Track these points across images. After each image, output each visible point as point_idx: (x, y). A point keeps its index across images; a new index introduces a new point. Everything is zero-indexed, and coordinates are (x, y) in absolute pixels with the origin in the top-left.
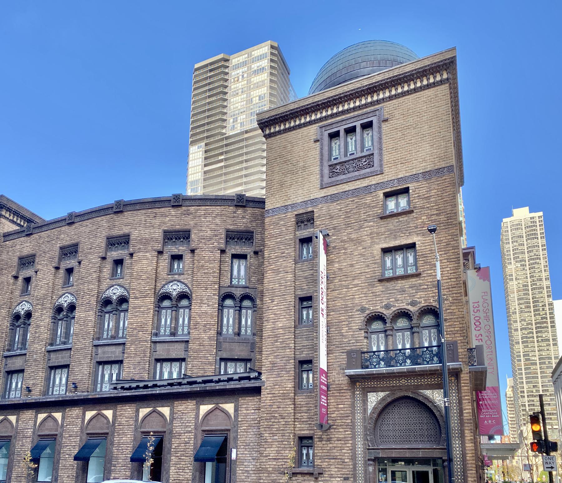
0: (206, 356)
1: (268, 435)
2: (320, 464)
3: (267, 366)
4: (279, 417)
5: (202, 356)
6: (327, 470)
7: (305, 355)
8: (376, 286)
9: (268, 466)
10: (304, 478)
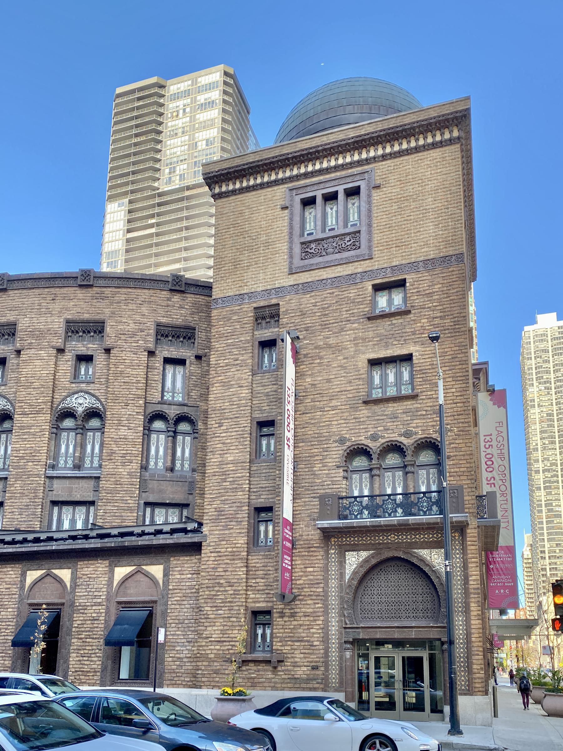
0: (125, 498)
1: (209, 609)
2: (280, 648)
3: (210, 514)
4: (225, 584)
5: (119, 498)
6: (289, 656)
7: (263, 500)
8: (361, 410)
9: (209, 652)
10: (259, 667)
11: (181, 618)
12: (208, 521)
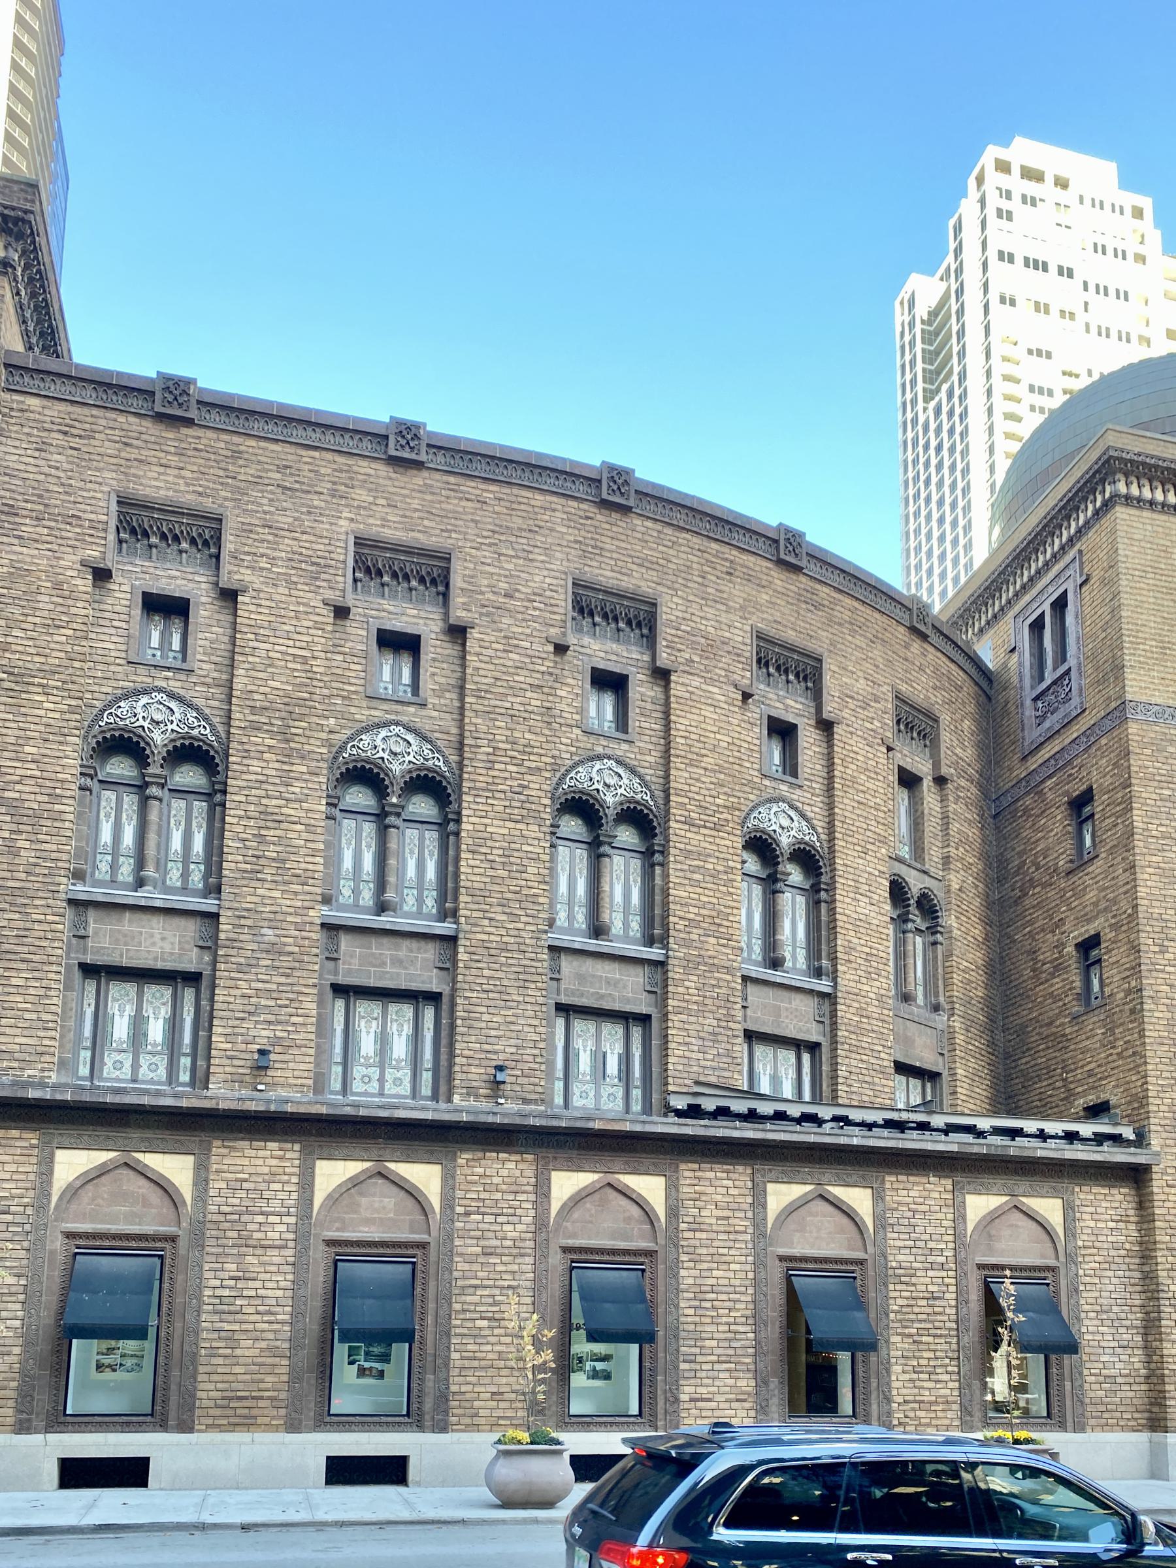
11: (1104, 1301)
12: (1159, 1128)
